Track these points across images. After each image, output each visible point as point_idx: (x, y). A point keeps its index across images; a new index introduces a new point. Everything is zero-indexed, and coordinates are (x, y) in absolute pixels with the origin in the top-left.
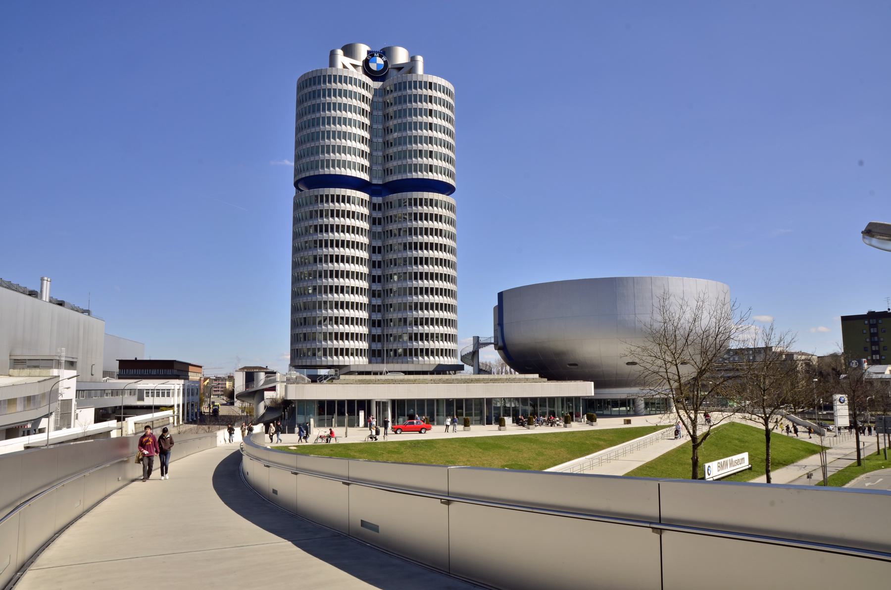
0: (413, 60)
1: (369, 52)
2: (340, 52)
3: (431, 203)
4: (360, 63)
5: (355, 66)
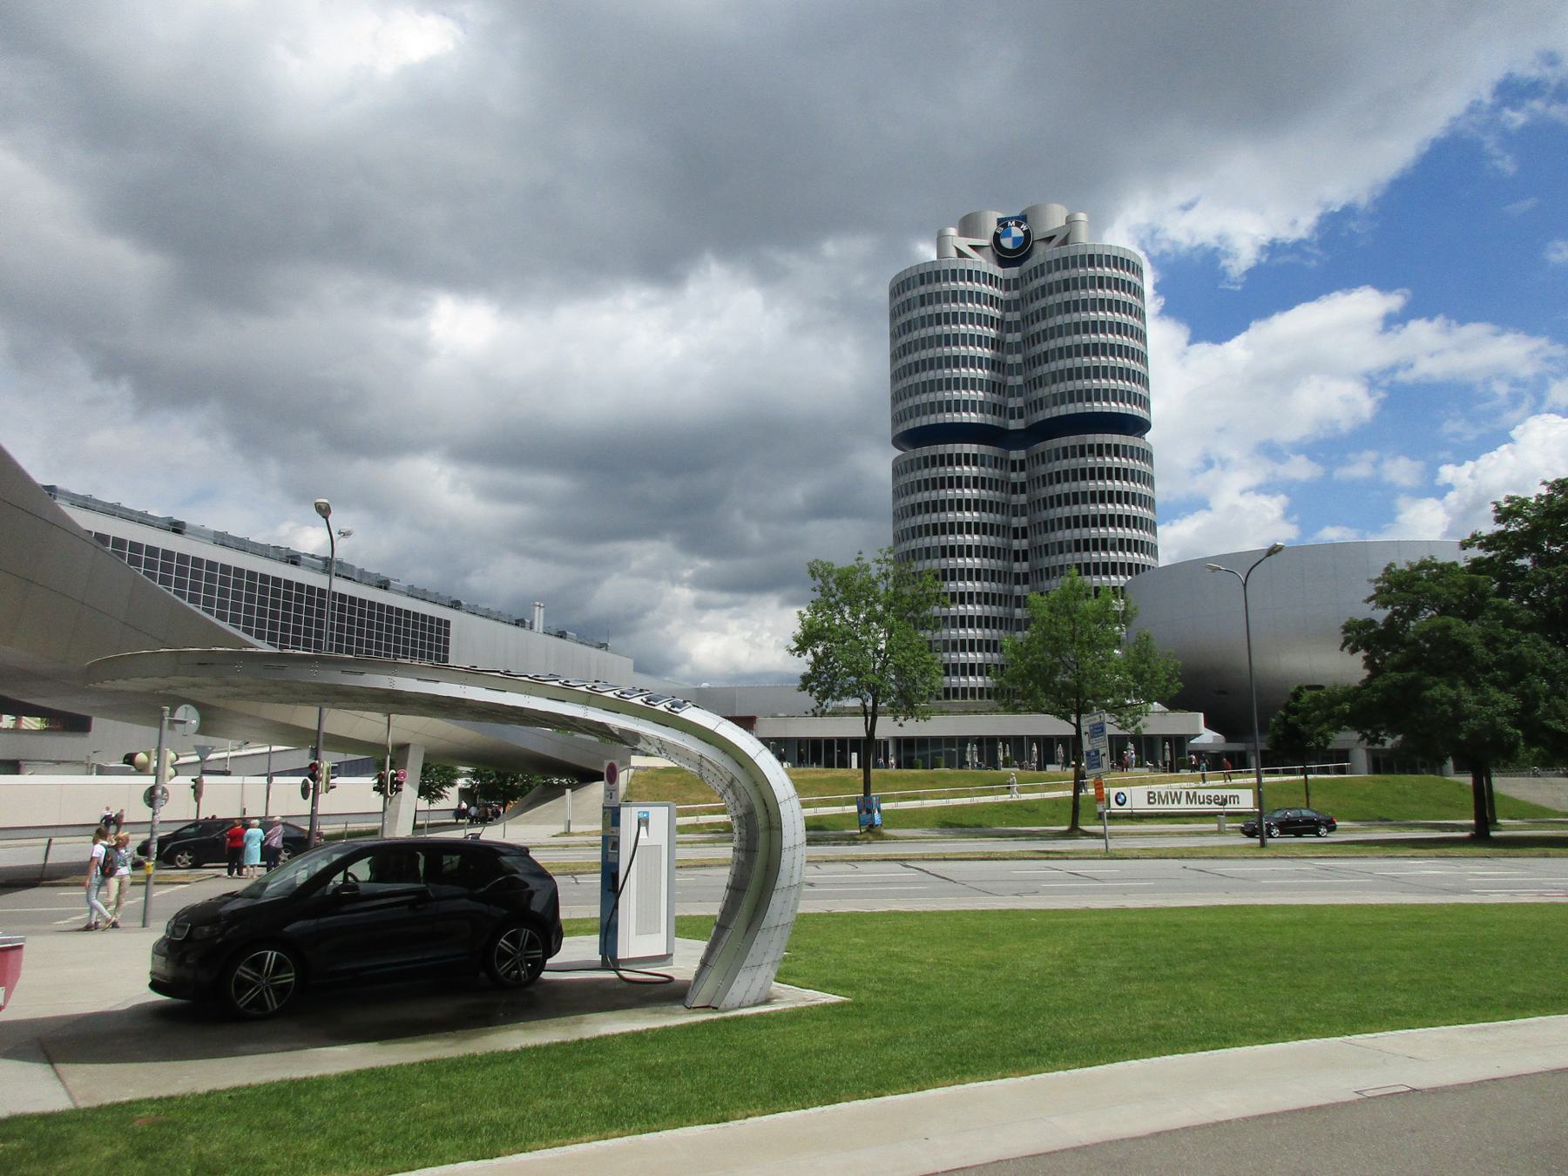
0: (1070, 221)
1: (1000, 221)
2: (952, 231)
3: (1100, 450)
4: (986, 241)
5: (973, 247)
